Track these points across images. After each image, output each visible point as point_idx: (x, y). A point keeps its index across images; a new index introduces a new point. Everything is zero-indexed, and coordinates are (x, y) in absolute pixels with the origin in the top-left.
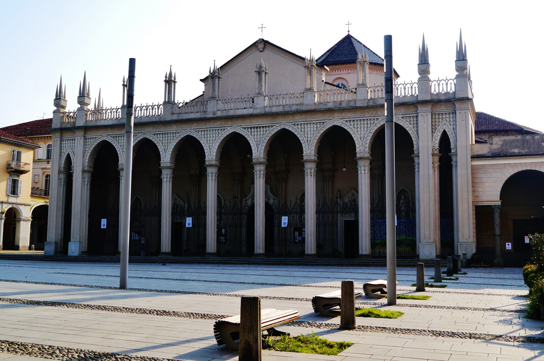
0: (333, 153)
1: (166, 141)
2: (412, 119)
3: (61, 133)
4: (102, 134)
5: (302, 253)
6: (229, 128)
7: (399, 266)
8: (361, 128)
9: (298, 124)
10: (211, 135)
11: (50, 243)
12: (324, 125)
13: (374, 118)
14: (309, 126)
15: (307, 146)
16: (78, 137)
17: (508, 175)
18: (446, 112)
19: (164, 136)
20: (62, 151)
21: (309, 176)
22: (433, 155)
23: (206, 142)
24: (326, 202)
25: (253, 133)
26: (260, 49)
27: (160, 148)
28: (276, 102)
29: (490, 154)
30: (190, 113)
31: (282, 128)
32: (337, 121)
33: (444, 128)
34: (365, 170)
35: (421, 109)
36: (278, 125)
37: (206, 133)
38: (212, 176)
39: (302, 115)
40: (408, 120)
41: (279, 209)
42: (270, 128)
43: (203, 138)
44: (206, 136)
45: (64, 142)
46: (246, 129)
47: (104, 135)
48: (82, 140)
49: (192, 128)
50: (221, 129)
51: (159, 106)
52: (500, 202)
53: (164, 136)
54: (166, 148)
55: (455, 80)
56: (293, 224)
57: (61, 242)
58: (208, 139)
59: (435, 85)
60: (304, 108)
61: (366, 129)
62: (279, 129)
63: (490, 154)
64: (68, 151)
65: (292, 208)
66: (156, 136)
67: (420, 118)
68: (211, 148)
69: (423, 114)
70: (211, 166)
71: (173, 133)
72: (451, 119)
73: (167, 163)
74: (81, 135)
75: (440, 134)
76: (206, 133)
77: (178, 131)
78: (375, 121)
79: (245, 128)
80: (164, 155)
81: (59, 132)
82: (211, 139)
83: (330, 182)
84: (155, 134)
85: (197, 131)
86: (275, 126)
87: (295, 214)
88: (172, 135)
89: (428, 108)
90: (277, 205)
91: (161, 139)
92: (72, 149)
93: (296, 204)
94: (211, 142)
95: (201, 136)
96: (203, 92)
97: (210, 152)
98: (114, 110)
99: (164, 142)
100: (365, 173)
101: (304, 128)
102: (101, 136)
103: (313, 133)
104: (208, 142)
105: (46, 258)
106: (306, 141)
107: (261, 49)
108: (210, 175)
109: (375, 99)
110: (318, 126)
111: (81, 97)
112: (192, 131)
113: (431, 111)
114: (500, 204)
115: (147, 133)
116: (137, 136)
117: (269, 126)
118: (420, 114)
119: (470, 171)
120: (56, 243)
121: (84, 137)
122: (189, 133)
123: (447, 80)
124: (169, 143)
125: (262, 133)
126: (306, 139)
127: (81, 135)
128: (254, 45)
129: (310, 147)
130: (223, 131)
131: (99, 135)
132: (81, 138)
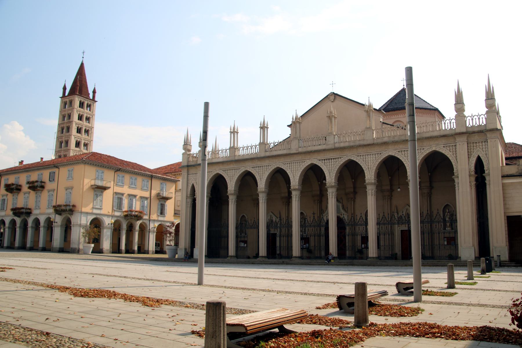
0: (390, 177)
1: (262, 172)
2: (451, 148)
6: (308, 161)
9: (360, 156)
10: (295, 167)
14: (369, 156)
18: (479, 141)
19: (260, 168)
21: (370, 196)
22: (470, 176)
23: (290, 172)
25: (326, 164)
30: (278, 150)
31: (349, 158)
35: (458, 139)
36: (345, 157)
37: (290, 165)
38: (296, 198)
39: (363, 148)
40: (448, 149)
42: (339, 159)
44: (290, 167)
50: (302, 162)
51: (256, 146)
53: (260, 168)
55: (486, 115)
57: (189, 249)
58: (292, 169)
59: (469, 120)
60: (365, 143)
62: (346, 159)
63: (517, 174)
66: (254, 168)
67: (458, 147)
69: (460, 143)
70: (294, 190)
72: (484, 147)
79: (320, 160)
82: (295, 169)
83: (389, 200)
84: (253, 167)
89: (464, 138)
91: (258, 171)
92: (195, 180)
94: (295, 171)
98: (224, 151)
103: (372, 162)
104: (293, 172)
109: (421, 133)
110: (377, 156)
112: (281, 164)
117: (338, 158)
118: (457, 144)
120: (185, 249)
123: (479, 116)
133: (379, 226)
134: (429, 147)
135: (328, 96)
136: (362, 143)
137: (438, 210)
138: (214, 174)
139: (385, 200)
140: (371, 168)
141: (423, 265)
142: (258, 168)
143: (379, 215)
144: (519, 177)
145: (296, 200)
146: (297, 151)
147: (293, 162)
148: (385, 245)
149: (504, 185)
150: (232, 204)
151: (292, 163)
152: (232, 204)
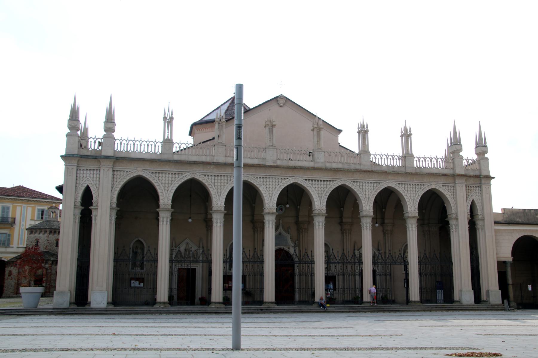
1: (219, 184)
2: (450, 188)
4: (137, 168)
5: (153, 302)
6: (290, 178)
7: (244, 313)
8: (411, 191)
11: (62, 293)
12: (380, 185)
13: (421, 184)
14: (367, 184)
15: (366, 202)
16: (104, 168)
17: (516, 239)
18: (473, 185)
19: (216, 178)
20: (78, 182)
21: (368, 230)
25: (314, 186)
26: (281, 104)
27: (212, 190)
28: (347, 160)
29: (503, 221)
31: (343, 183)
32: (391, 183)
33: (473, 198)
36: (339, 181)
37: (265, 180)
39: (361, 174)
40: (447, 188)
41: (429, 260)
42: (331, 182)
43: (262, 185)
45: (82, 172)
46: (308, 181)
47: (139, 169)
48: (111, 172)
49: (250, 174)
50: (282, 178)
52: (512, 259)
53: (216, 178)
54: (219, 191)
58: (267, 186)
61: (414, 192)
62: (340, 184)
64: (88, 183)
65: (396, 259)
67: (458, 188)
68: (271, 195)
69: (460, 185)
70: (367, 216)
71: (227, 176)
74: (109, 166)
76: (265, 180)
78: (422, 186)
79: (306, 180)
80: (218, 198)
81: (78, 159)
82: (271, 186)
84: (205, 175)
85: (255, 177)
86: (335, 181)
88: (226, 178)
90: (298, 255)
91: (213, 181)
92: (93, 181)
94: (271, 189)
95: (259, 182)
97: (271, 200)
98: (124, 142)
99: (216, 184)
100: (412, 230)
101: (266, 181)
102: (136, 170)
103: (370, 191)
104: (268, 190)
105: (64, 311)
106: (365, 198)
107: (281, 105)
108: (267, 223)
110: (375, 185)
111: (109, 123)
112: (250, 176)
113: (465, 183)
114: (512, 260)
115: (196, 173)
116: (184, 175)
118: (457, 185)
119: (494, 234)
121: (113, 168)
123: (437, 159)
124: (222, 187)
125: (322, 186)
126: (364, 196)
127: (109, 166)
128: (276, 99)
129: (369, 204)
130: (283, 180)
131: (133, 168)
132: (109, 170)
133: (374, 265)
134: (429, 184)
135: (278, 99)
136: (358, 167)
138: (132, 176)
139: (345, 235)
140: (369, 198)
142: (213, 177)
144: (507, 225)
145: (272, 228)
146: (274, 163)
150: (167, 224)
151: (266, 178)
152: (167, 224)
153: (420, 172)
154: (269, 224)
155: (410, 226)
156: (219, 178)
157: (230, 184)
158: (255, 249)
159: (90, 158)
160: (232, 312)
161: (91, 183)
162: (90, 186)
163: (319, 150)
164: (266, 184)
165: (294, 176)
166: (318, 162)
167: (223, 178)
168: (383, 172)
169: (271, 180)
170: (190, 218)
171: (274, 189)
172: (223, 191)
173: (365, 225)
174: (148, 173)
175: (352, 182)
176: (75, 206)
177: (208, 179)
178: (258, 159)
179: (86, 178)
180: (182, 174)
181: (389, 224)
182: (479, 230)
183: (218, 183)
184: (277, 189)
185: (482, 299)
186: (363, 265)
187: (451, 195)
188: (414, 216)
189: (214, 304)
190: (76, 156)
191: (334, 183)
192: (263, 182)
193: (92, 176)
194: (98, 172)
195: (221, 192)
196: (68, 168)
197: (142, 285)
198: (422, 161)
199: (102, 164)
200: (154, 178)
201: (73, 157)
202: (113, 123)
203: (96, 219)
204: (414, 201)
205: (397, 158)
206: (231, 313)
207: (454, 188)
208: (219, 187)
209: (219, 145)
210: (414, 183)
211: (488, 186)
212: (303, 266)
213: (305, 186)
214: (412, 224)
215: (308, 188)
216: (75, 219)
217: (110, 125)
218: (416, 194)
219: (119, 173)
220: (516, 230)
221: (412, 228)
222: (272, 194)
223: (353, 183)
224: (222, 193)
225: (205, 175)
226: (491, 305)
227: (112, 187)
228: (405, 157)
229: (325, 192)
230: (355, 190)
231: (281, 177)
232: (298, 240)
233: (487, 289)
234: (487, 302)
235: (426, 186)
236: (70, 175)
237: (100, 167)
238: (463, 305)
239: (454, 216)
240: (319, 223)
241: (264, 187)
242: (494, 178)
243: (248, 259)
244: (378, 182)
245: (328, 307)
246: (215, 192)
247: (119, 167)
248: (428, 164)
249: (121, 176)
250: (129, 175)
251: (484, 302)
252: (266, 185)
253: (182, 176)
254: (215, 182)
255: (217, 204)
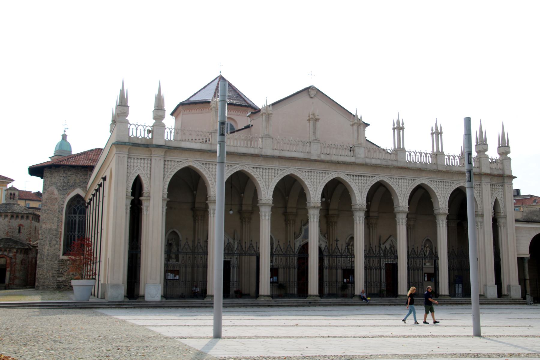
1: (267, 177)
3: (166, 152)
6: (334, 173)
9: (394, 178)
13: (451, 181)
16: (155, 158)
17: (533, 236)
19: (264, 171)
24: (200, 243)
31: (381, 179)
33: (496, 196)
34: (443, 224)
35: (484, 179)
36: (378, 176)
37: (310, 174)
42: (371, 178)
43: (308, 179)
45: (132, 161)
46: (349, 176)
47: (190, 159)
50: (325, 173)
52: (529, 255)
53: (264, 171)
54: (267, 184)
56: (339, 267)
63: (522, 220)
64: (139, 172)
67: (484, 186)
69: (485, 183)
71: (275, 169)
73: (269, 201)
74: (161, 156)
75: (494, 201)
76: (310, 174)
77: (281, 168)
78: (452, 184)
79: (348, 175)
80: (266, 191)
82: (315, 180)
84: (253, 168)
86: (374, 177)
87: (335, 257)
88: (273, 171)
91: (261, 174)
92: (144, 170)
93: (251, 246)
94: (315, 184)
96: (366, 137)
97: (316, 194)
100: (443, 226)
102: (187, 161)
108: (312, 216)
110: (410, 182)
116: (234, 167)
118: (483, 183)
122: (292, 172)
127: (161, 156)
131: (184, 158)
132: (160, 159)
134: (458, 182)
136: (395, 163)
137: (279, 241)
139: (371, 229)
140: (404, 194)
141: (225, 306)
142: (261, 170)
143: (342, 245)
144: (526, 223)
147: (313, 171)
148: (185, 281)
149: (517, 228)
151: (311, 172)
153: (450, 170)
154: (314, 218)
155: (441, 222)
156: (267, 171)
157: (277, 177)
158: (371, 244)
159: (142, 147)
160: (213, 306)
161: (141, 172)
162: (141, 176)
163: (360, 146)
164: (311, 178)
165: (337, 171)
166: (359, 158)
167: (270, 171)
168: (418, 170)
169: (315, 175)
170: (231, 210)
171: (318, 183)
172: (271, 184)
173: (401, 221)
174: (199, 163)
175: (389, 179)
176: (127, 197)
177: (257, 171)
178: (303, 152)
179: (137, 167)
180: (231, 166)
181: (413, 219)
182: (501, 227)
183: (266, 175)
184: (321, 183)
185: (503, 293)
186: (399, 260)
187: (477, 193)
188: (445, 212)
189: (263, 297)
190: (128, 144)
191: (373, 179)
192: (308, 176)
193: (142, 165)
194: (149, 162)
195: (269, 185)
196: (119, 156)
197: (177, 277)
198: (452, 159)
199: (153, 153)
200: (204, 169)
201: (125, 145)
202: (164, 111)
203: (147, 210)
204: (404, 196)
205: (429, 155)
206: (212, 307)
207: (480, 187)
208: (267, 180)
209: (267, 137)
210: (445, 181)
211: (511, 185)
212: (373, 261)
213: (347, 181)
214: (442, 221)
215: (350, 183)
216: (126, 209)
217: (160, 113)
218: (446, 191)
219: (170, 163)
220: (533, 227)
221: (443, 224)
222: (317, 188)
223: (391, 179)
224: (270, 187)
225: (253, 168)
226: (513, 299)
227: (164, 178)
228: (437, 155)
229: (365, 187)
230: (393, 186)
231: (325, 172)
232: (327, 233)
233: (508, 284)
234: (508, 296)
235: (456, 184)
236: (121, 164)
237: (151, 157)
238: (488, 299)
239: (480, 213)
240: (359, 217)
241: (309, 180)
242: (515, 177)
243: (282, 252)
244: (413, 178)
245: (369, 300)
246: (264, 185)
247: (170, 156)
248: (419, 159)
249: (172, 166)
250: (180, 166)
251: (505, 297)
252: (311, 179)
253: (232, 168)
254: (263, 175)
255: (266, 197)
